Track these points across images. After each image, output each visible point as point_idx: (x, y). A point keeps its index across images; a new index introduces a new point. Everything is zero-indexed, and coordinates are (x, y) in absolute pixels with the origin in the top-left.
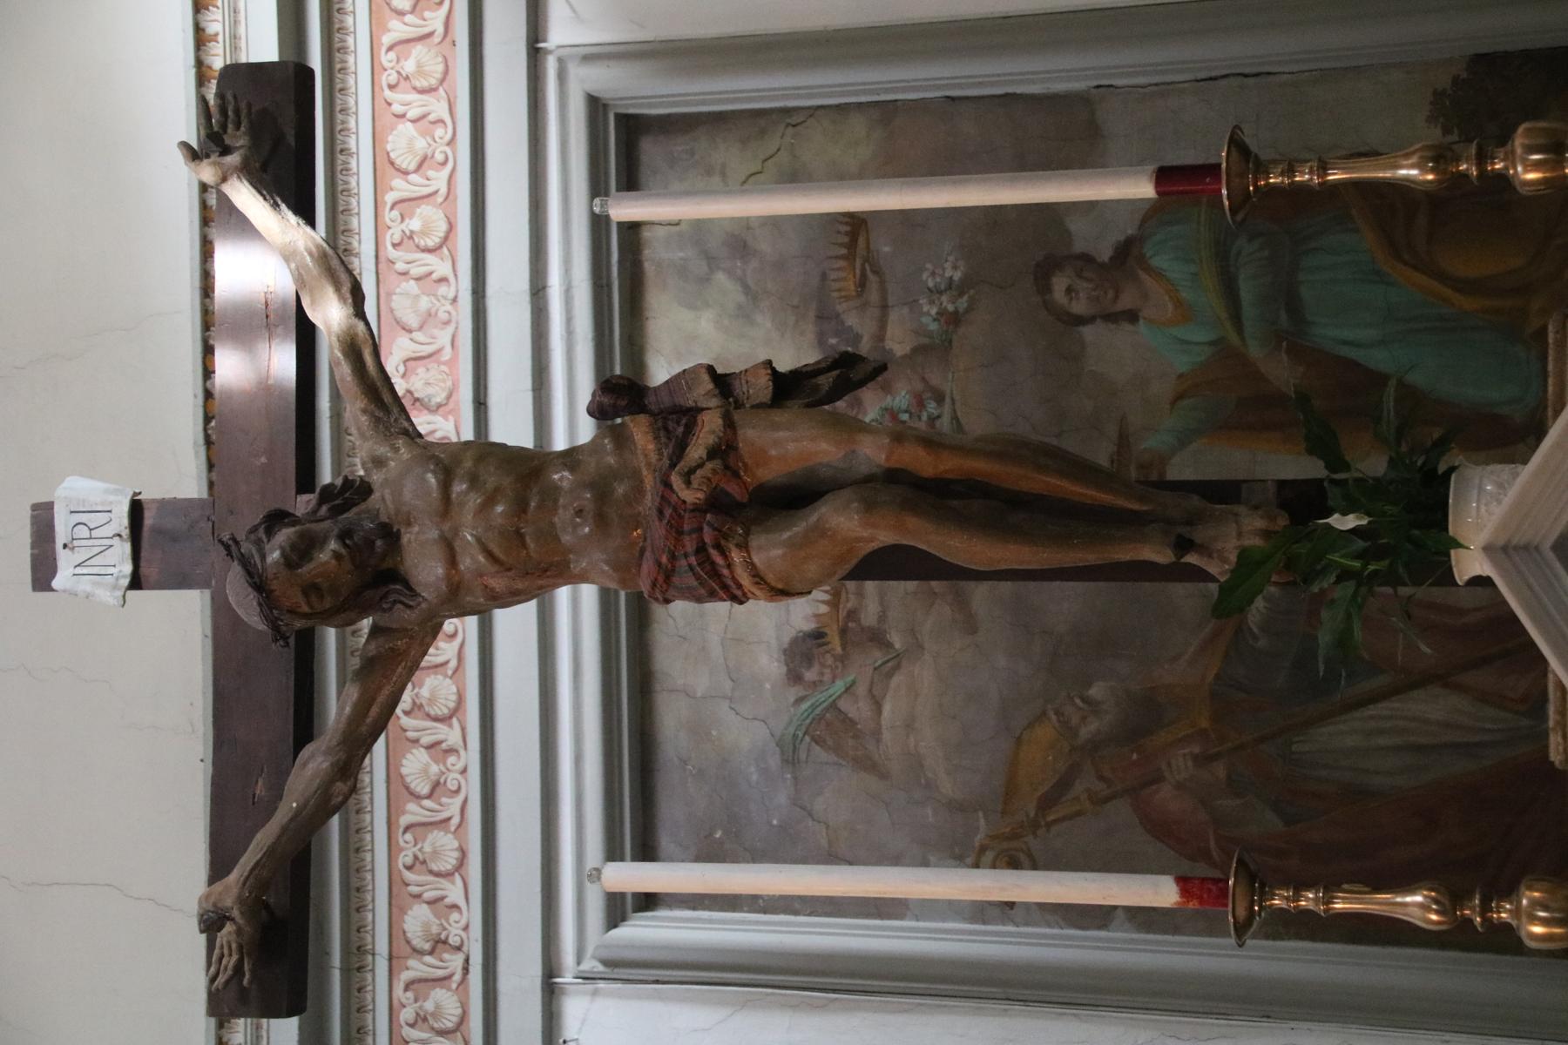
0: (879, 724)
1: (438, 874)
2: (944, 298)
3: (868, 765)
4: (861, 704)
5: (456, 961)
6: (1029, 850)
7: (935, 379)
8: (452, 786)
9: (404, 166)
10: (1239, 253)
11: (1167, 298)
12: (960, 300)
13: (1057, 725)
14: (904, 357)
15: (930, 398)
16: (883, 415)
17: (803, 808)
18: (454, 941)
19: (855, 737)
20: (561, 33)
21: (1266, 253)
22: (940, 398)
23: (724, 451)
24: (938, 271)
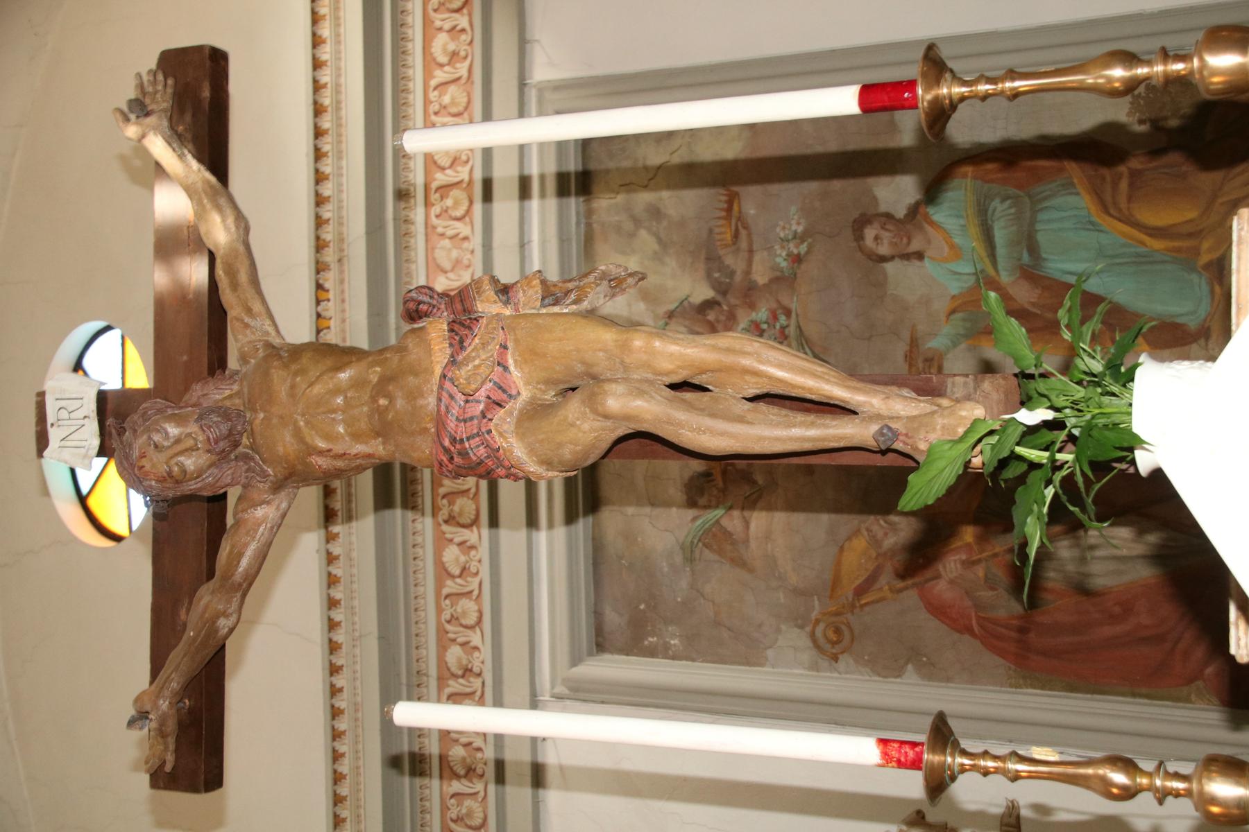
0: (747, 535)
1: (466, 627)
2: (791, 245)
3: (740, 562)
4: (735, 521)
5: (477, 683)
6: (848, 623)
7: (786, 301)
8: (473, 570)
9: (443, 164)
10: (994, 211)
11: (944, 242)
12: (801, 246)
13: (867, 538)
14: (764, 285)
15: (781, 314)
16: (750, 326)
17: (698, 591)
18: (476, 670)
19: (732, 544)
21: (1013, 211)
22: (788, 313)
24: (787, 226)
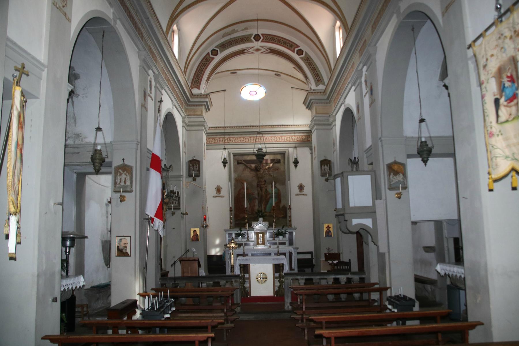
3: (243, 170)
20: (290, 149)
23: (263, 187)
